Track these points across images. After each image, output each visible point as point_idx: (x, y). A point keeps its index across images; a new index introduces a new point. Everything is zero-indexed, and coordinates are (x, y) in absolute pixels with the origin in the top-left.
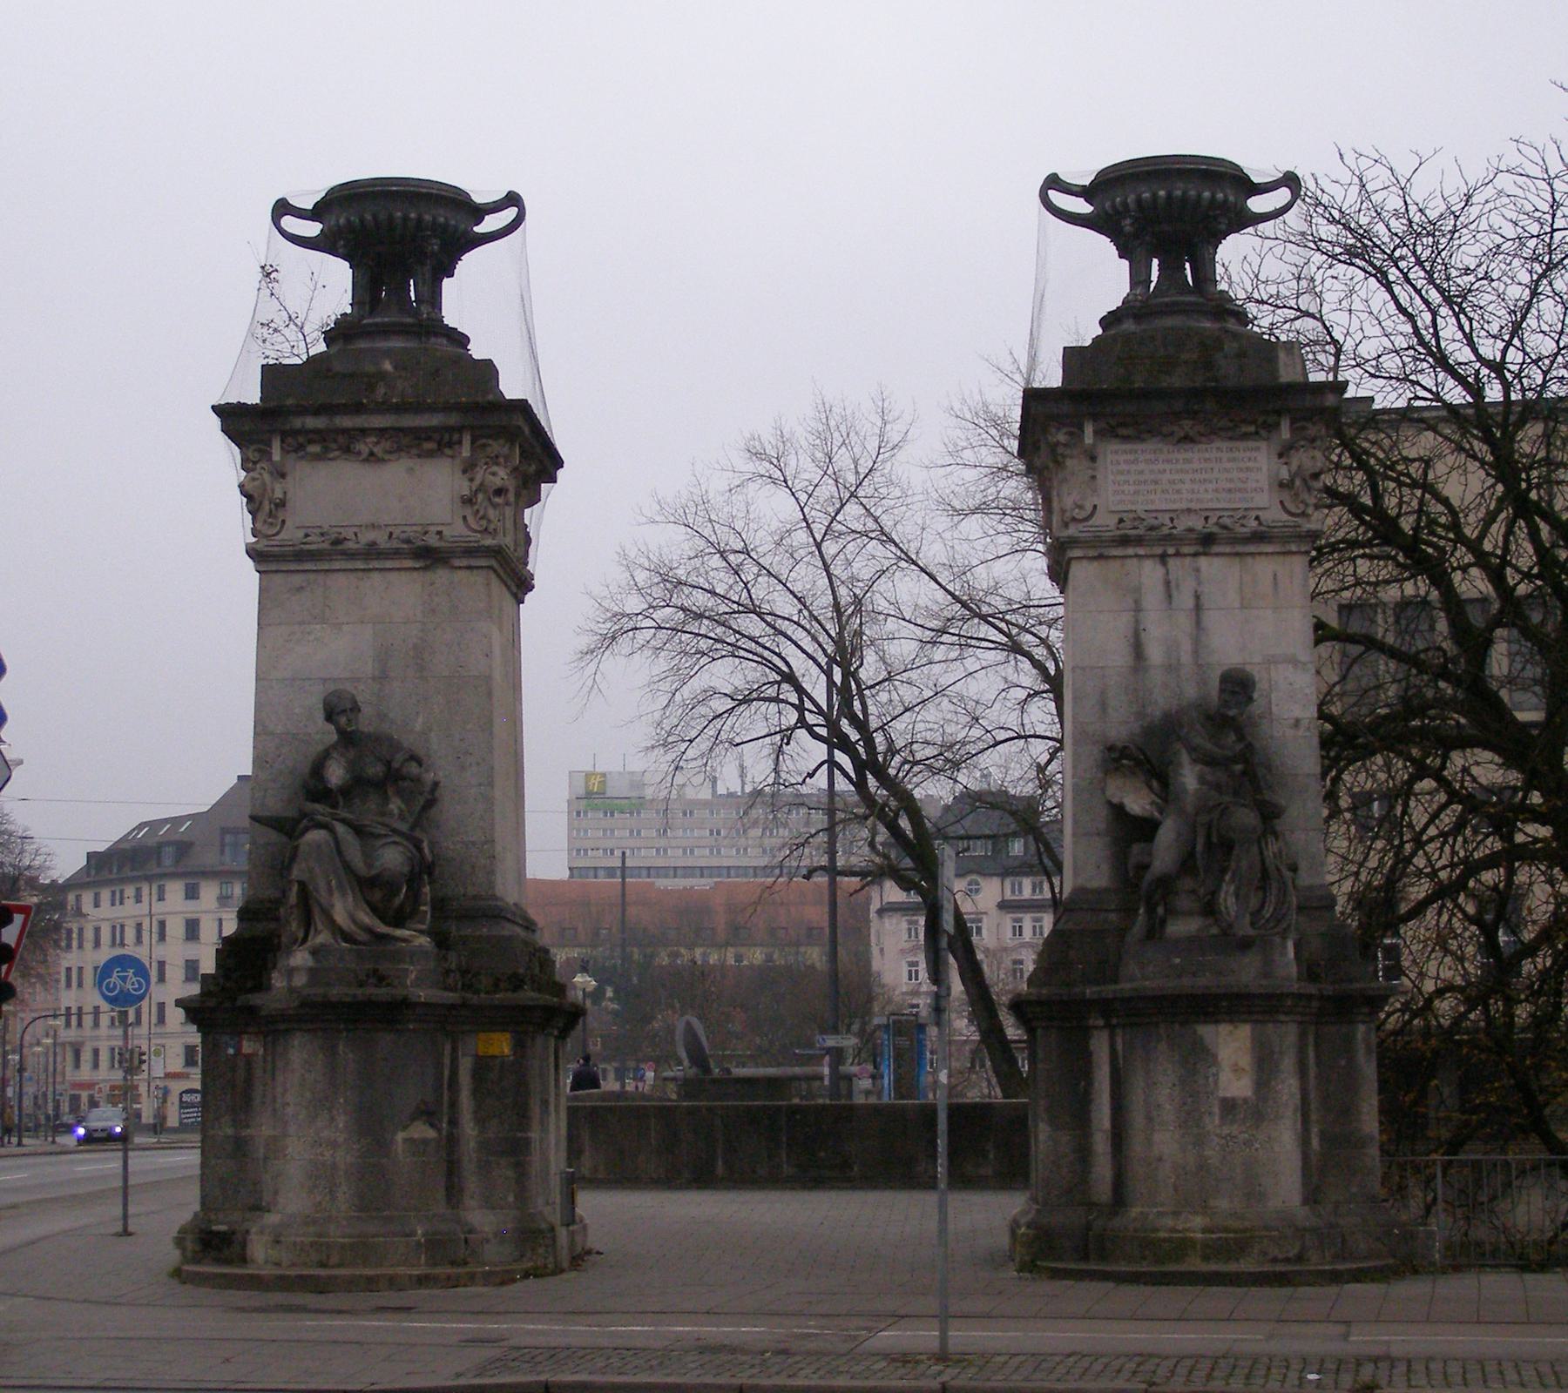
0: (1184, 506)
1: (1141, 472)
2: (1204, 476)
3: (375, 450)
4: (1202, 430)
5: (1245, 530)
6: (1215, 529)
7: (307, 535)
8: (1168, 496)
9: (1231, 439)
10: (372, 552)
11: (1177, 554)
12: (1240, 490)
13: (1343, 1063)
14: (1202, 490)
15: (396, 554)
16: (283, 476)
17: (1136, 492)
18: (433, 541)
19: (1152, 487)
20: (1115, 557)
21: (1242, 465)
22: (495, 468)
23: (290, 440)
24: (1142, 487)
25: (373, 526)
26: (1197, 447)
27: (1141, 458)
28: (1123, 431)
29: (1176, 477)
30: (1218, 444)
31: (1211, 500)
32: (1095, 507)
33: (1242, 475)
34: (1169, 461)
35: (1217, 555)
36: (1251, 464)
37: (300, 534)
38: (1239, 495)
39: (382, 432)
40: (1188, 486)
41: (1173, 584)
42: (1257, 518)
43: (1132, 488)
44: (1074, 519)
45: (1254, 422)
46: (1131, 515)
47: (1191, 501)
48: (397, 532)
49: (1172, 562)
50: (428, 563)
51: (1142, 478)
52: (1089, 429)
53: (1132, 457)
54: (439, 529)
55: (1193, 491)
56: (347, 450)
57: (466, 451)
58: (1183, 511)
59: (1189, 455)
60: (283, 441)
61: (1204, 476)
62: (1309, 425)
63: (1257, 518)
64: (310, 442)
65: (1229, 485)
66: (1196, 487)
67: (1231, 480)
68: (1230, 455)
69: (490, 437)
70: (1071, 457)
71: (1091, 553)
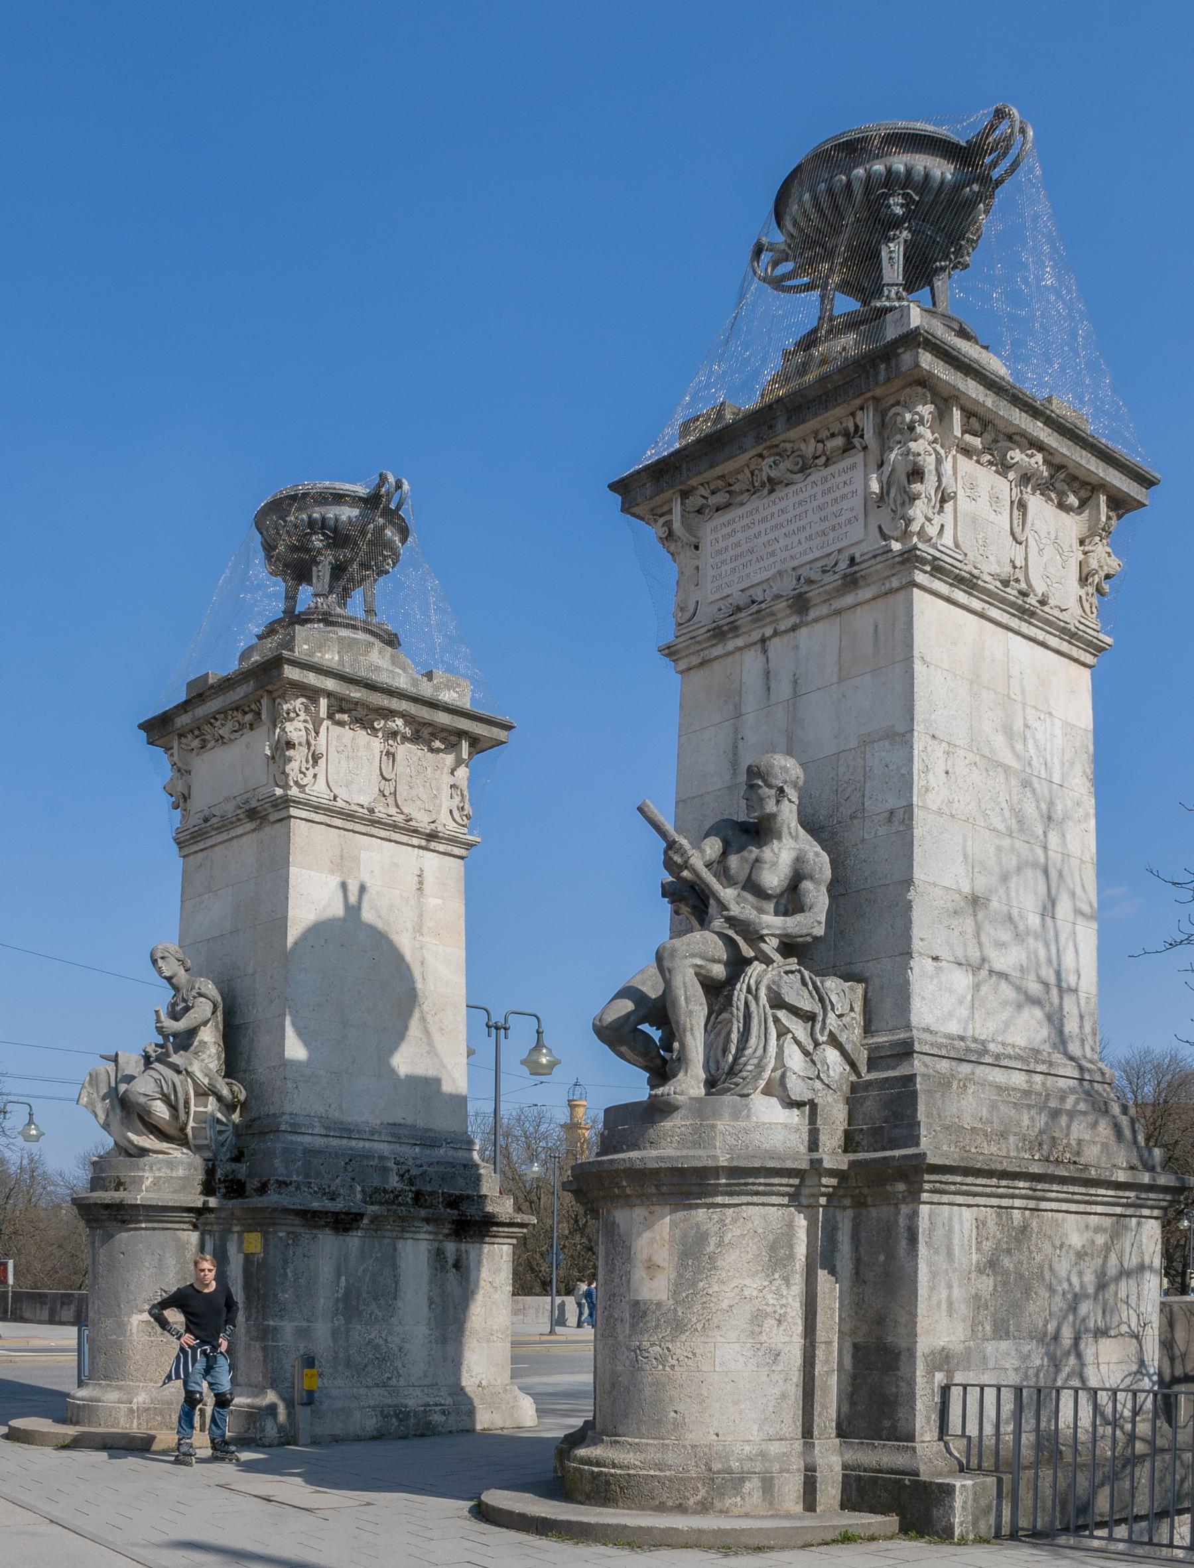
11: (776, 633)
13: (882, 1258)
20: (716, 658)
31: (805, 553)
34: (765, 520)
35: (816, 620)
41: (772, 675)
49: (775, 645)
51: (739, 550)
53: (728, 530)
61: (799, 524)
71: (695, 660)
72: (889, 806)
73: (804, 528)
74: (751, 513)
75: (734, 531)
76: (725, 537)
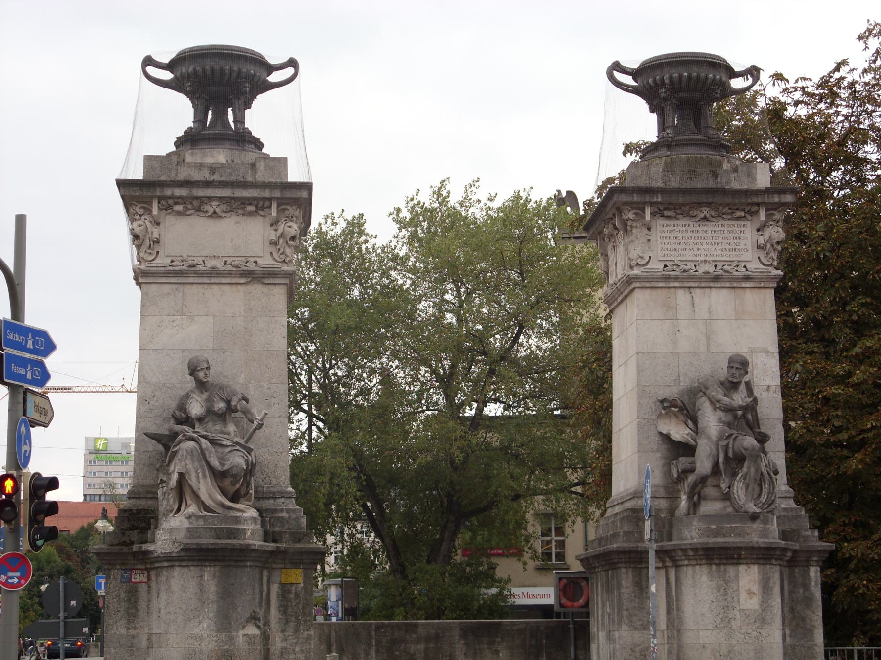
0: (703, 258)
1: (677, 238)
2: (713, 241)
3: (217, 210)
4: (713, 214)
5: (737, 273)
6: (721, 272)
7: (172, 261)
8: (692, 252)
9: (729, 219)
10: (214, 273)
12: (735, 250)
14: (713, 249)
15: (229, 274)
16: (158, 224)
17: (675, 250)
18: (252, 267)
19: (684, 246)
21: (736, 235)
22: (290, 224)
23: (164, 203)
24: (678, 247)
25: (215, 256)
26: (710, 224)
27: (678, 229)
28: (666, 213)
29: (699, 241)
30: (721, 222)
32: (650, 257)
33: (736, 241)
34: (693, 232)
36: (741, 235)
37: (168, 261)
38: (734, 253)
39: (221, 199)
40: (705, 246)
42: (745, 267)
43: (672, 247)
44: (638, 264)
45: (744, 210)
46: (672, 263)
47: (707, 255)
48: (229, 260)
50: (249, 279)
51: (678, 241)
52: (648, 212)
53: (672, 229)
54: (256, 259)
55: (708, 250)
56: (198, 210)
57: (274, 212)
58: (702, 261)
59: (705, 228)
60: (159, 203)
62: (775, 212)
63: (745, 267)
64: (176, 203)
65: (729, 247)
66: (709, 247)
67: (730, 244)
68: (730, 229)
69: (287, 204)
70: (636, 227)
72: (768, 383)
73: (718, 244)
74: (685, 225)
75: (674, 230)
76: (668, 231)
